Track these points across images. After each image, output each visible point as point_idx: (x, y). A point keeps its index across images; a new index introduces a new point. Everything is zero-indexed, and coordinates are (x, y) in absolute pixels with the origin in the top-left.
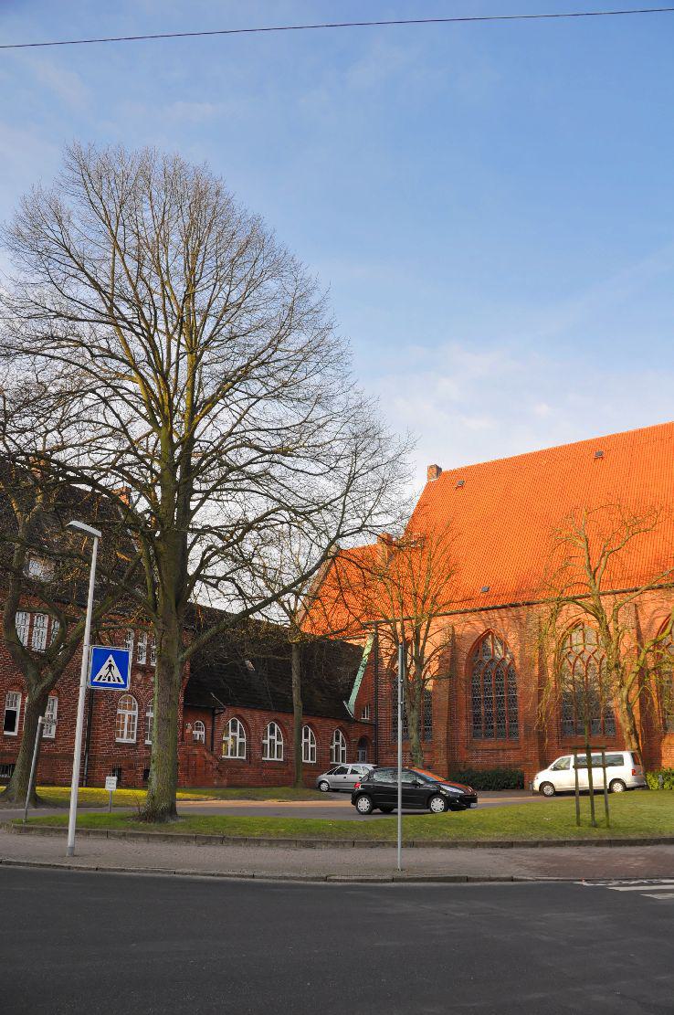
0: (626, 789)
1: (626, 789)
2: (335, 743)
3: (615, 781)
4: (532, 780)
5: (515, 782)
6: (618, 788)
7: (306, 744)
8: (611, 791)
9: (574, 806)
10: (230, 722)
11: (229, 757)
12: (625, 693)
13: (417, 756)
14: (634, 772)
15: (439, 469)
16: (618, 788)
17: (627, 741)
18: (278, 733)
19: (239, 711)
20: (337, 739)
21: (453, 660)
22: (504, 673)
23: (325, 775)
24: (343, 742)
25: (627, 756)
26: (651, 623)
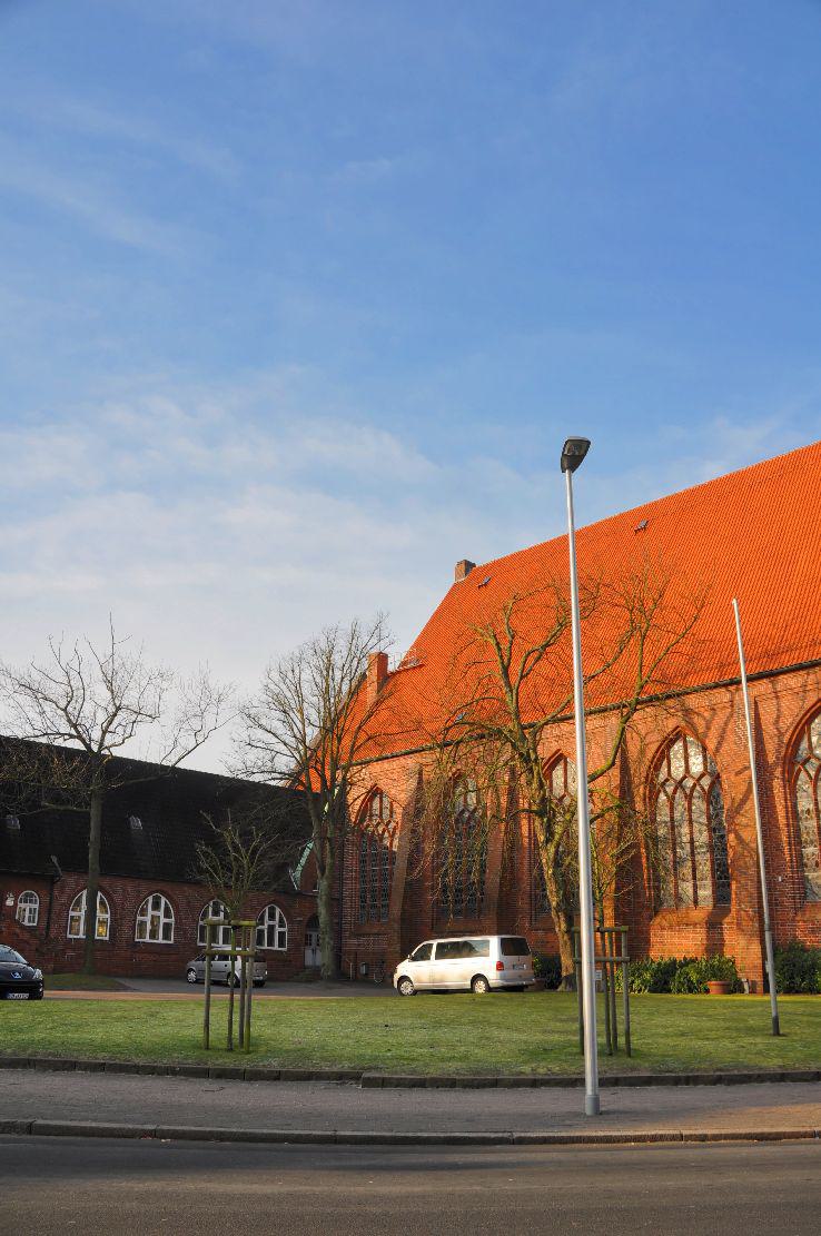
0: (489, 989)
1: (489, 989)
2: (267, 922)
3: (477, 978)
4: (395, 971)
5: (372, 976)
6: (480, 987)
7: (271, 928)
8: (471, 990)
9: (631, 1009)
10: (150, 899)
11: (147, 940)
12: (552, 850)
13: (324, 939)
14: (500, 966)
15: (469, 566)
16: (480, 987)
17: (556, 920)
18: (167, 909)
19: (160, 886)
20: (272, 917)
21: (419, 812)
22: (468, 825)
23: (193, 962)
24: (281, 920)
25: (494, 942)
26: (642, 752)
